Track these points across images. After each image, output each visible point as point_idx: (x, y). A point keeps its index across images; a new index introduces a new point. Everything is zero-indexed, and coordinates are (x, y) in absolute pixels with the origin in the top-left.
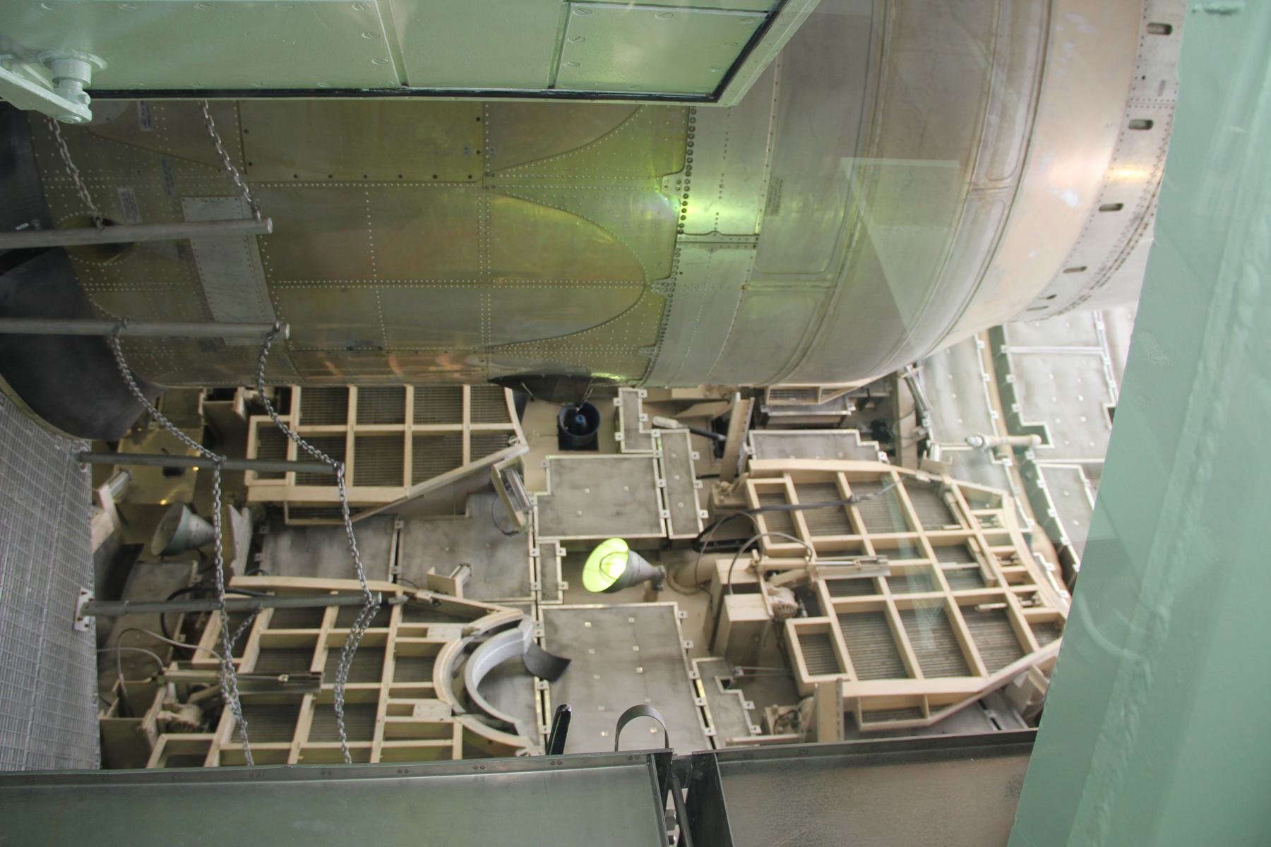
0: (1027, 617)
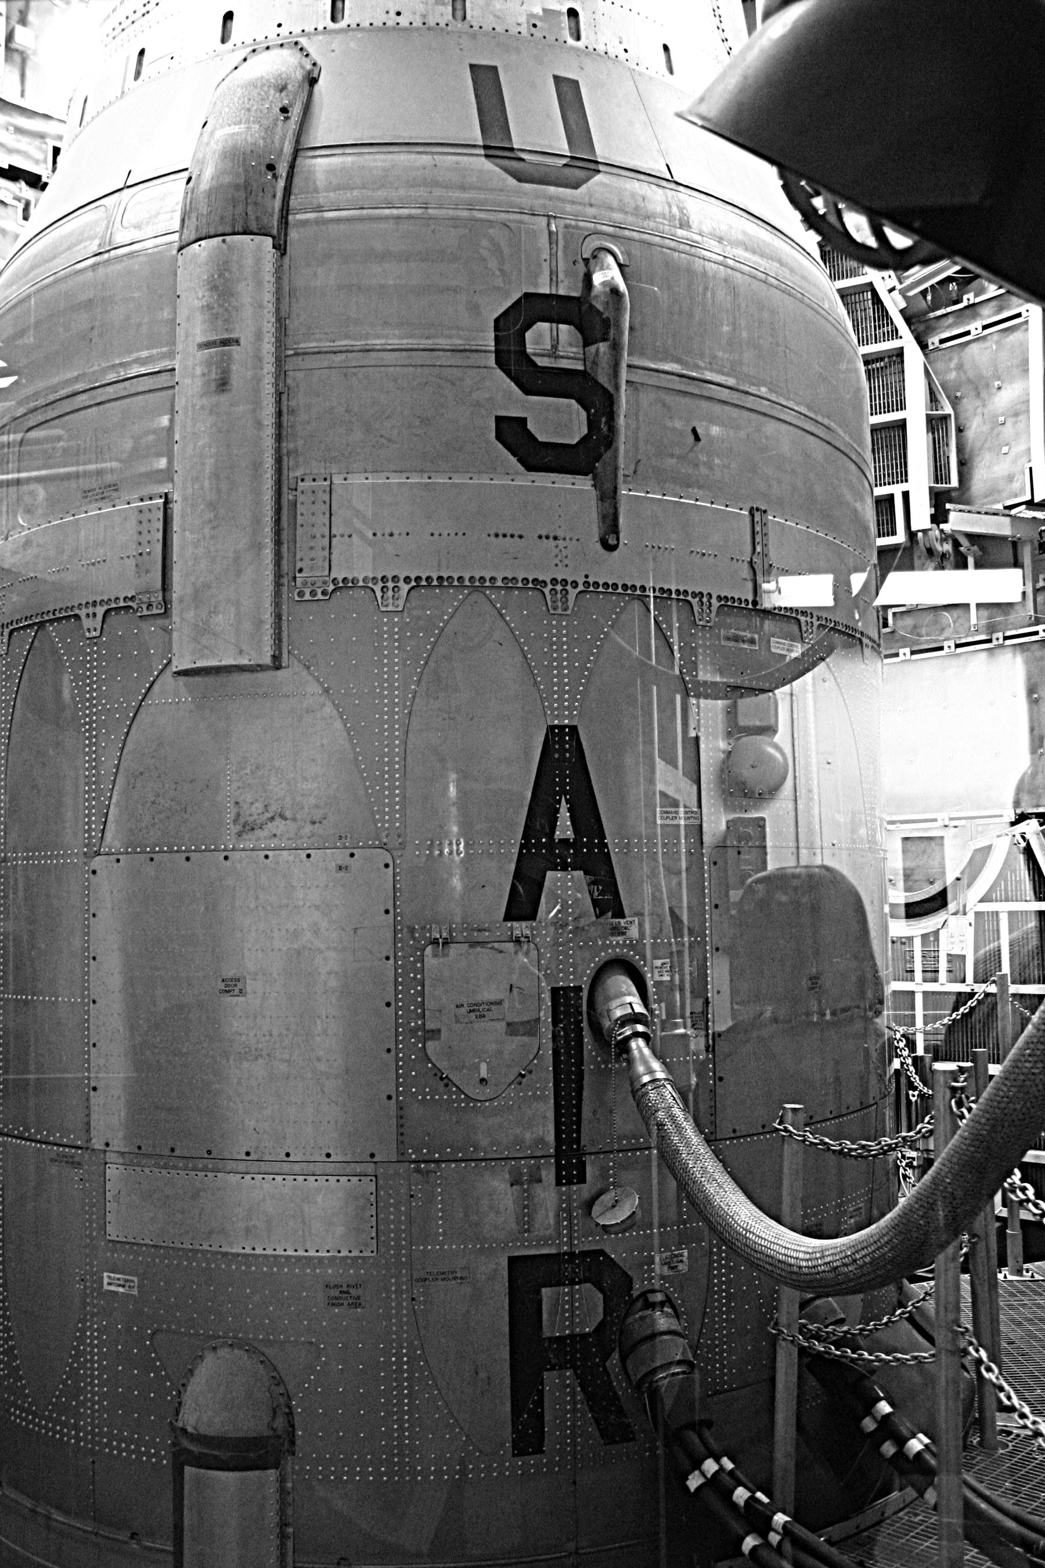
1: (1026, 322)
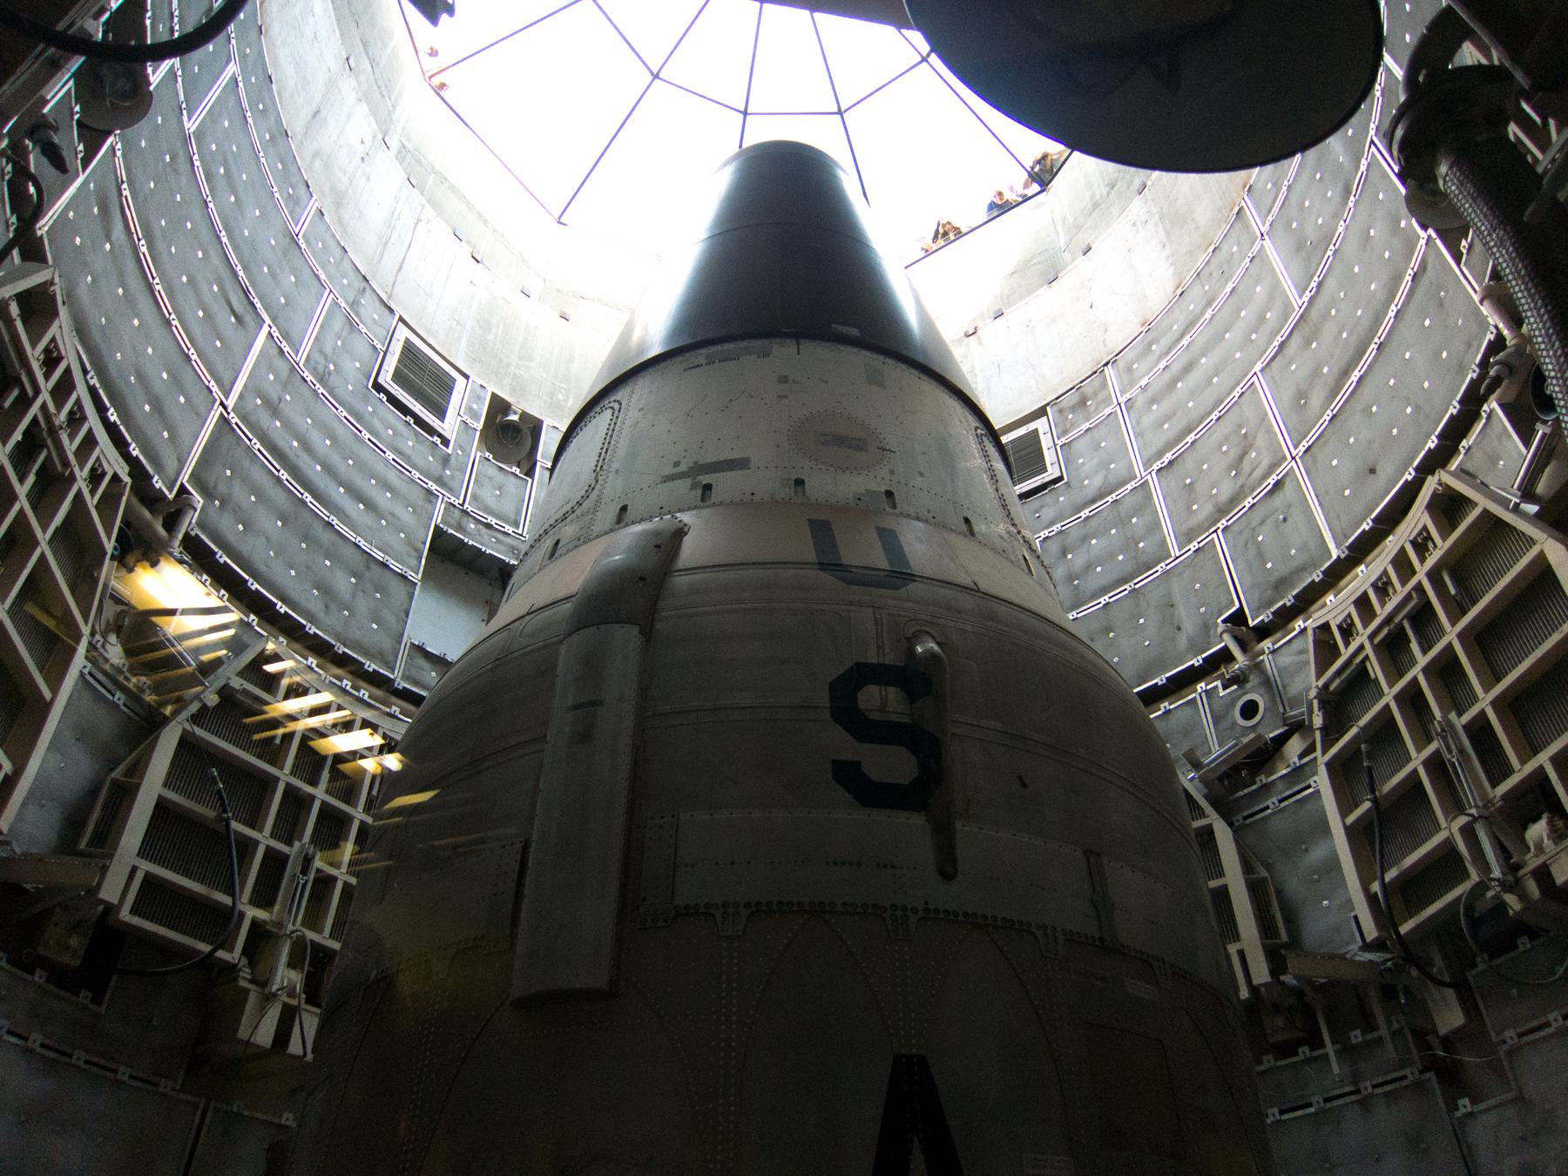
0: (1444, 539)
1: (1318, 792)
